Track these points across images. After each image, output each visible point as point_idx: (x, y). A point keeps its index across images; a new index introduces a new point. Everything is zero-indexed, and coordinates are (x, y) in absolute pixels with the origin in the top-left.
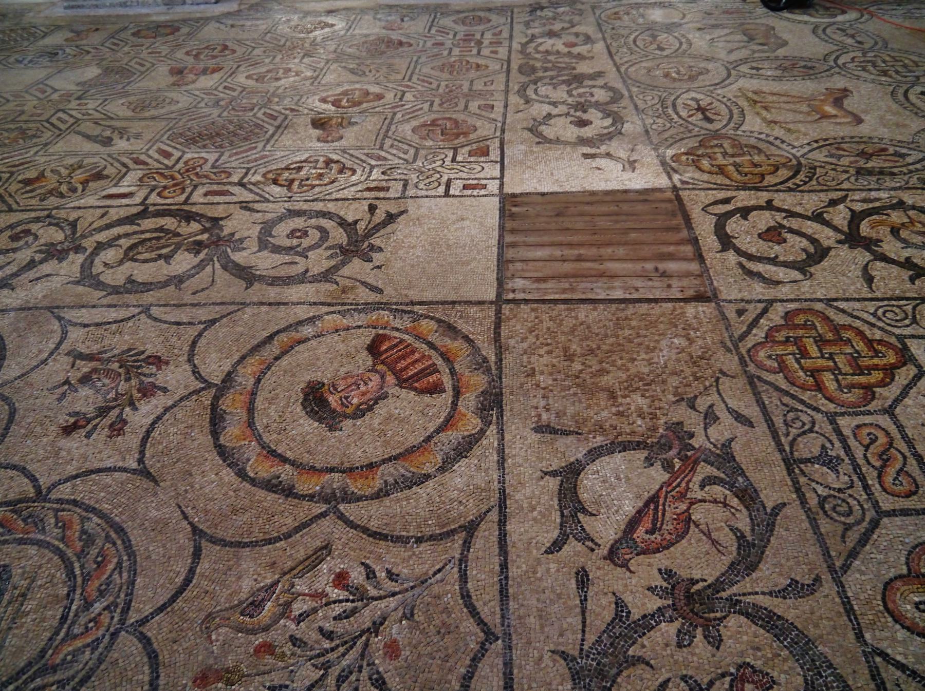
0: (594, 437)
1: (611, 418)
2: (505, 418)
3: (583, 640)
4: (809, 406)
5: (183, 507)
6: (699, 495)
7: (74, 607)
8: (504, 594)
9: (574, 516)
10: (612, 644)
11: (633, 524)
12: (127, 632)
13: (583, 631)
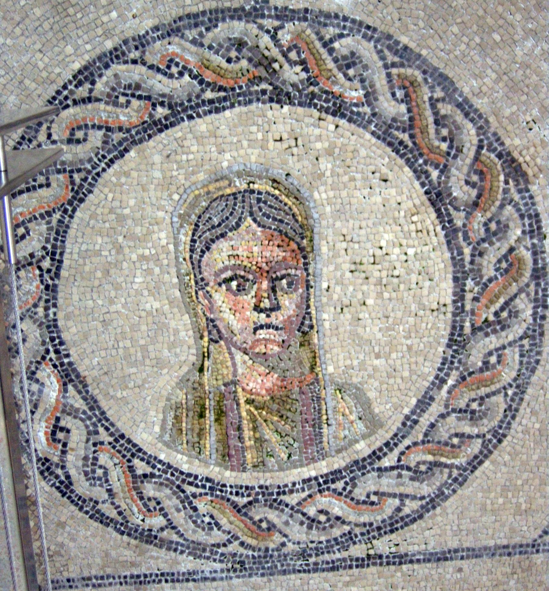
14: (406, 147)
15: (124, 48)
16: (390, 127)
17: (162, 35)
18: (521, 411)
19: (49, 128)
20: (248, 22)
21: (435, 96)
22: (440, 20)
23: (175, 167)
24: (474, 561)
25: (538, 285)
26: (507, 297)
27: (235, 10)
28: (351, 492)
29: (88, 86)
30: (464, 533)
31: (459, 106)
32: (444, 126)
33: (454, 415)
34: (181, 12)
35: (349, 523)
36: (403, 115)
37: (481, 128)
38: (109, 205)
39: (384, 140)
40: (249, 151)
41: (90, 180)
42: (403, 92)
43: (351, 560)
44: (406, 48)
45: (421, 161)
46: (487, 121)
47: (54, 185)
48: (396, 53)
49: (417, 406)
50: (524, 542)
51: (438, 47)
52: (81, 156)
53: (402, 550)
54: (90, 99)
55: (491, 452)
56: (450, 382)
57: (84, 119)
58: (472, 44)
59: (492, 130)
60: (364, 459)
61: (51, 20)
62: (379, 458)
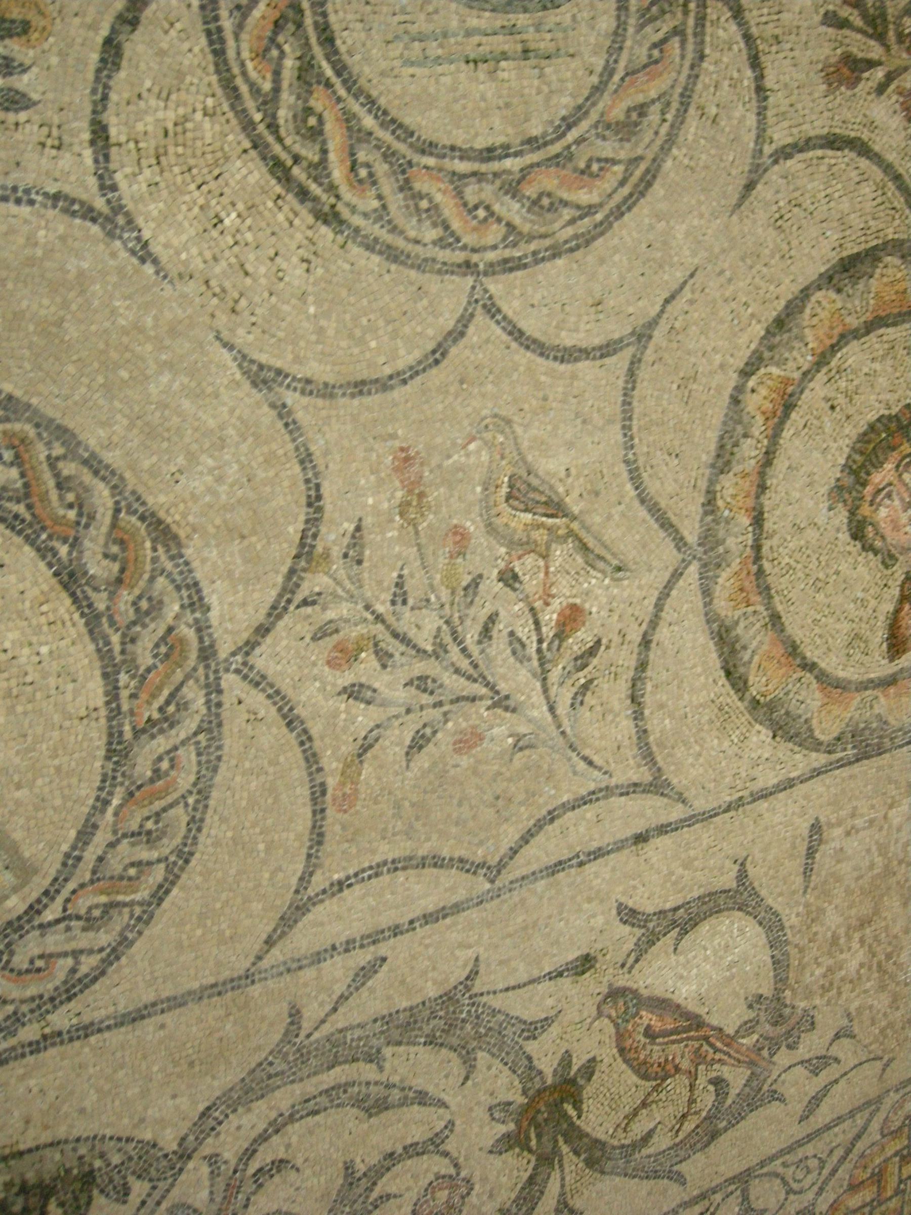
0: (798, 915)
1: (829, 929)
2: (837, 772)
3: (495, 992)
4: (825, 1182)
5: (691, 282)
6: (701, 1081)
7: (508, 163)
8: (558, 866)
9: (674, 924)
10: (490, 1029)
11: (661, 1005)
12: (473, 288)
13: (507, 989)
14: (23, 521)
18: (208, 820)
22: (51, 360)
24: (178, 1011)
25: (207, 667)
26: (173, 687)
28: (8, 962)
30: (160, 980)
31: (85, 462)
32: (69, 489)
33: (126, 841)
35: (13, 1001)
36: (15, 482)
37: (115, 487)
43: (23, 1046)
45: (44, 536)
46: (122, 478)
49: (78, 839)
50: (236, 975)
51: (51, 393)
53: (86, 1019)
55: (178, 877)
56: (116, 802)
59: (130, 488)
60: (19, 918)
62: (39, 912)
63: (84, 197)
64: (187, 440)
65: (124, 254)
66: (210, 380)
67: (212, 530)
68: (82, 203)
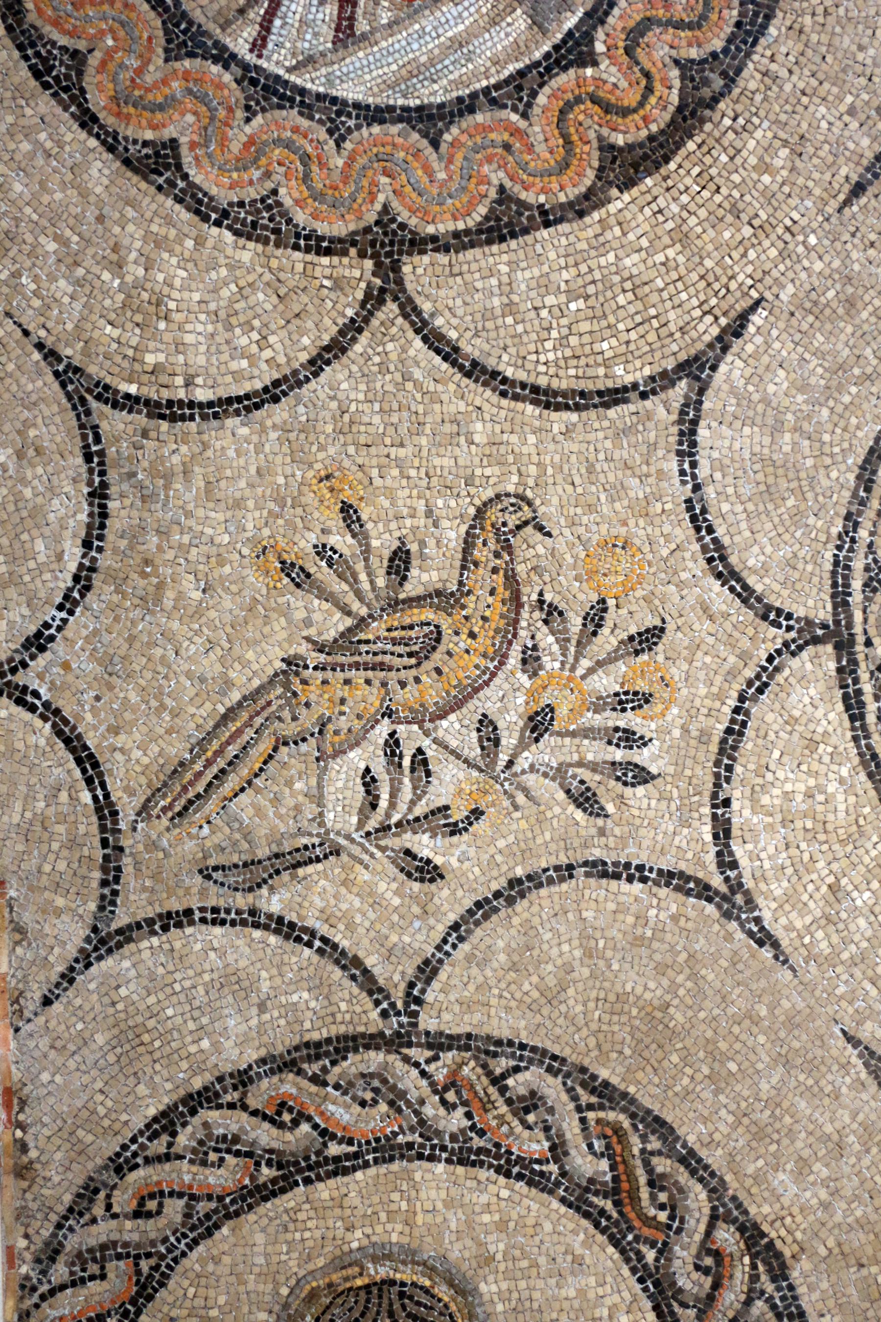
14: (608, 1218)
15: (218, 1087)
16: (587, 1190)
17: (271, 1069)
19: (108, 1196)
20: (389, 1052)
21: (649, 1147)
23: (285, 1250)
27: (372, 1036)
29: (165, 1138)
31: (683, 1160)
32: (662, 1189)
34: (296, 1041)
36: (605, 1173)
38: (188, 1303)
39: (578, 1209)
40: (389, 1227)
41: (163, 1269)
42: (603, 1142)
44: (606, 1084)
45: (630, 1237)
46: (722, 1180)
47: (111, 1275)
48: (593, 1091)
52: (153, 1235)
54: (167, 1157)
57: (159, 1183)
58: (699, 1077)
59: (731, 1192)
61: (119, 1050)
63: (700, 875)
64: (799, 1144)
65: (740, 935)
66: (830, 1077)
67: (823, 1252)
68: (698, 881)
